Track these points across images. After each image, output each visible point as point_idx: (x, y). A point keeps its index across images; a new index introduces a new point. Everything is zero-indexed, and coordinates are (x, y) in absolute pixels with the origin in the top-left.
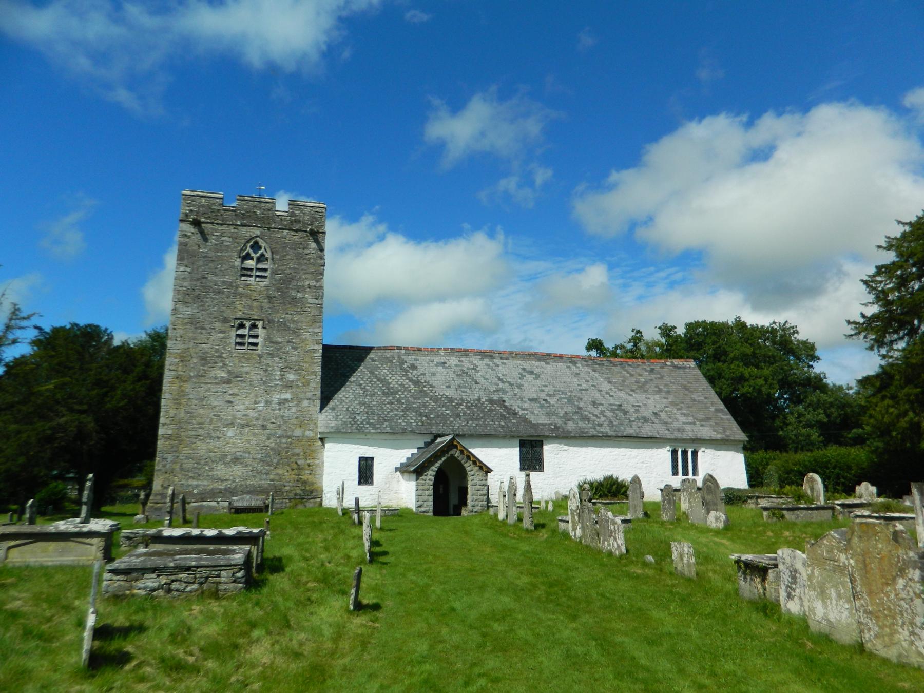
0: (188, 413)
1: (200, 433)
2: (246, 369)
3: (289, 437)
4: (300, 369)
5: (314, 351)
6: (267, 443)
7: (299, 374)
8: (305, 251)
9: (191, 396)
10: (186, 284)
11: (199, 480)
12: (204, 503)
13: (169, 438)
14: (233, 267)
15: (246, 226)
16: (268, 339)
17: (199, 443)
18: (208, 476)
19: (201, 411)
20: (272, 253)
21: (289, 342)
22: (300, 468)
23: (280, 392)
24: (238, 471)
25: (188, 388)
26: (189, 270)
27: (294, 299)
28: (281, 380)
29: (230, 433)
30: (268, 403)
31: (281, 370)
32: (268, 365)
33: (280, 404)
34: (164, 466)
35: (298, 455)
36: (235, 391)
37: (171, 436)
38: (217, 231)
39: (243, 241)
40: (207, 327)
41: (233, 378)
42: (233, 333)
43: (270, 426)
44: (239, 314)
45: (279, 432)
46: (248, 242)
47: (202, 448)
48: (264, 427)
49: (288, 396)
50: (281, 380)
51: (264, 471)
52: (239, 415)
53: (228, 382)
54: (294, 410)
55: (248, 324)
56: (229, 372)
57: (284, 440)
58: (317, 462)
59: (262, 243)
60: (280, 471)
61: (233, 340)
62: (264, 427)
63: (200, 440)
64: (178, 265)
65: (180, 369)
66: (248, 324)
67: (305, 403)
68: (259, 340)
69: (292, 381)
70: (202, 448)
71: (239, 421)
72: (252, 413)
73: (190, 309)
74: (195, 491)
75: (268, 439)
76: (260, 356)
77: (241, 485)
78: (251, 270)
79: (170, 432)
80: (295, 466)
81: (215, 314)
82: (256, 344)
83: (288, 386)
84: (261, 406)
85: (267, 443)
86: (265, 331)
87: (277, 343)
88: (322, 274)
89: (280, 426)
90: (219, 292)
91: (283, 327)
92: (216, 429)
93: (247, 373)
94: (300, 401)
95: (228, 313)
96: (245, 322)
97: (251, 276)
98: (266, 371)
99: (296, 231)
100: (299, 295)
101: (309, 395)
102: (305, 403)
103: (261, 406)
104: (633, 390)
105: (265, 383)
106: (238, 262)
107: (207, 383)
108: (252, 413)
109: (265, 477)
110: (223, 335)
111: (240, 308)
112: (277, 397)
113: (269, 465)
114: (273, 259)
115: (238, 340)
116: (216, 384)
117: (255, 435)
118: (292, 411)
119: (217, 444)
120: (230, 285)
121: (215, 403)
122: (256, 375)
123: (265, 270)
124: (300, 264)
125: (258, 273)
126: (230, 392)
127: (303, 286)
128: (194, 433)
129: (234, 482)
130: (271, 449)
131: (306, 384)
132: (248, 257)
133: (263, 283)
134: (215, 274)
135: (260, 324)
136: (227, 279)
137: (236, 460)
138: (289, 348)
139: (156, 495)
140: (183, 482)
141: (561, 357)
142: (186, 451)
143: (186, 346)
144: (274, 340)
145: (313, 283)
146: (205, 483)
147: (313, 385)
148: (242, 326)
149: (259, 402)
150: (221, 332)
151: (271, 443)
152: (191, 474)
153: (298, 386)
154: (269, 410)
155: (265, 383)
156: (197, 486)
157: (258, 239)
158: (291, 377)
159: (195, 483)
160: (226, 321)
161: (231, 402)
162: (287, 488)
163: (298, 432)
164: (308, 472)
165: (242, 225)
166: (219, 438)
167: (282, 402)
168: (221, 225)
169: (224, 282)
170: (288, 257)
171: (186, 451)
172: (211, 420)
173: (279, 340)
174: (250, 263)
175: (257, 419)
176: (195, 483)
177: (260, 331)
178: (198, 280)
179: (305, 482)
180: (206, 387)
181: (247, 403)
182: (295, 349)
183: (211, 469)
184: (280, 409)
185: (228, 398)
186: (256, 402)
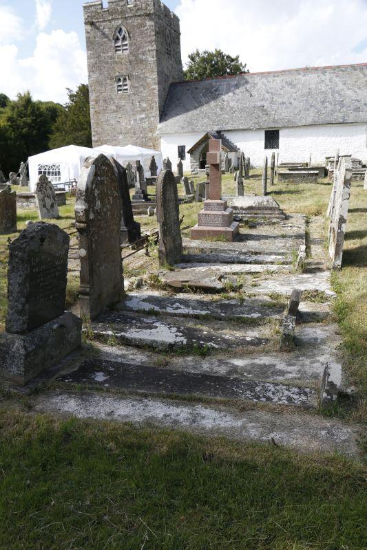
2: (123, 104)
3: (146, 138)
5: (154, 89)
8: (146, 28)
16: (132, 86)
19: (107, 127)
27: (142, 61)
29: (121, 137)
30: (135, 120)
39: (114, 29)
40: (104, 83)
42: (116, 85)
44: (117, 74)
45: (141, 135)
49: (144, 116)
53: (117, 112)
56: (117, 107)
59: (123, 29)
61: (116, 89)
67: (152, 119)
78: (120, 46)
82: (127, 89)
83: (143, 110)
84: (132, 122)
90: (107, 63)
94: (150, 118)
97: (120, 50)
99: (139, 16)
100: (144, 57)
101: (153, 114)
102: (152, 119)
103: (132, 122)
104: (359, 88)
105: (133, 110)
111: (119, 71)
112: (139, 117)
114: (129, 37)
115: (119, 88)
117: (131, 137)
118: (146, 125)
120: (111, 58)
123: (126, 45)
124: (143, 38)
125: (124, 48)
132: (117, 39)
133: (126, 52)
134: (104, 53)
136: (110, 54)
141: (316, 69)
148: (119, 80)
153: (148, 110)
158: (144, 105)
160: (112, 79)
167: (142, 119)
168: (103, 22)
170: (137, 34)
173: (137, 85)
174: (119, 44)
175: (131, 129)
180: (107, 115)
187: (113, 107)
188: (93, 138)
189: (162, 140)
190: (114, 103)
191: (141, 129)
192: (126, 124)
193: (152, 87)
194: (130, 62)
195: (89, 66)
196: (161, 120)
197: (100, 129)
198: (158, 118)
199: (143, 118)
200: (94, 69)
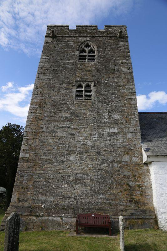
0: (42, 142)
1: (49, 157)
2: (83, 112)
3: (120, 162)
4: (122, 111)
6: (102, 167)
7: (123, 115)
9: (44, 130)
10: (46, 64)
11: (46, 195)
12: (50, 218)
13: (27, 160)
14: (74, 55)
15: (81, 36)
16: (98, 93)
17: (48, 165)
18: (54, 193)
19: (51, 141)
20: (98, 48)
21: (112, 94)
22: (131, 189)
23: (110, 127)
24: (79, 189)
25: (42, 125)
26: (48, 58)
27: (113, 71)
28: (109, 118)
29: (72, 158)
30: (101, 135)
31: (109, 112)
32: (99, 109)
33: (110, 136)
34: (21, 183)
35: (128, 177)
36: (76, 126)
37: (28, 159)
38: (65, 39)
39: (80, 43)
40: (57, 86)
41: (75, 116)
42: (74, 90)
43: (103, 153)
44: (78, 79)
45: (111, 158)
46: (83, 43)
47: (50, 170)
48: (98, 154)
49: (116, 130)
50: (109, 118)
51: (101, 191)
52: (78, 144)
53: (71, 120)
54: (121, 141)
55: (84, 85)
56: (71, 113)
57: (115, 165)
58: (145, 184)
59: (90, 43)
60: (115, 192)
62: (98, 154)
63: (49, 163)
64: (42, 56)
65: (38, 112)
66: (84, 85)
67: (130, 136)
68: (92, 93)
69: (118, 120)
70: (50, 170)
71: (79, 149)
72: (89, 143)
73: (47, 77)
74: (43, 206)
75: (103, 163)
76: (93, 103)
77: (82, 203)
79: (27, 156)
80: (127, 187)
81: (63, 79)
82: (90, 96)
83: (115, 123)
85: (102, 167)
86: (95, 88)
87: (104, 95)
88: (129, 56)
89: (111, 153)
91: (108, 85)
92: (62, 155)
93: (84, 114)
94: (125, 134)
95: (72, 79)
96: (82, 83)
98: (98, 112)
99: (110, 37)
101: (131, 130)
102: (130, 136)
103: (95, 137)
105: (98, 121)
106: (77, 53)
107: (56, 121)
108: (89, 143)
109: (101, 196)
110: (67, 91)
112: (107, 131)
113: (105, 186)
116: (62, 121)
117: (92, 160)
119: (61, 166)
121: (61, 135)
122: (91, 116)
126: (72, 127)
127: (118, 63)
128: (44, 157)
129: (75, 199)
130: (106, 172)
131: (128, 121)
135: (92, 85)
137: (77, 180)
138: (113, 98)
139: (13, 206)
140: (35, 197)
142: (39, 171)
143: (43, 98)
144: (102, 93)
145: (124, 61)
146: (52, 199)
147: (133, 122)
149: (94, 135)
150: (66, 89)
151: (105, 167)
152: (41, 191)
153: (122, 123)
154: (102, 140)
155: (98, 121)
156: (45, 201)
157: (88, 42)
158: (116, 116)
159: (44, 198)
160: (69, 83)
161: (73, 135)
162: (122, 207)
163: (126, 158)
164: (138, 192)
165: (79, 36)
166: (63, 162)
167: (111, 135)
169: (68, 63)
171: (39, 171)
172: (58, 147)
175: (93, 147)
176: (44, 198)
177: (93, 88)
178: (53, 62)
179: (137, 202)
181: (85, 135)
182: (117, 98)
183: (57, 187)
184: (110, 140)
185: (70, 131)
186: (91, 135)
187: (66, 115)
188: (22, 155)
189: (153, 169)
190: (68, 109)
191: (110, 148)
192: (85, 139)
193: (129, 97)
194: (98, 70)
195: (40, 68)
196: (144, 139)
197: (37, 142)
198: (139, 136)
199: (115, 133)
200: (46, 72)
